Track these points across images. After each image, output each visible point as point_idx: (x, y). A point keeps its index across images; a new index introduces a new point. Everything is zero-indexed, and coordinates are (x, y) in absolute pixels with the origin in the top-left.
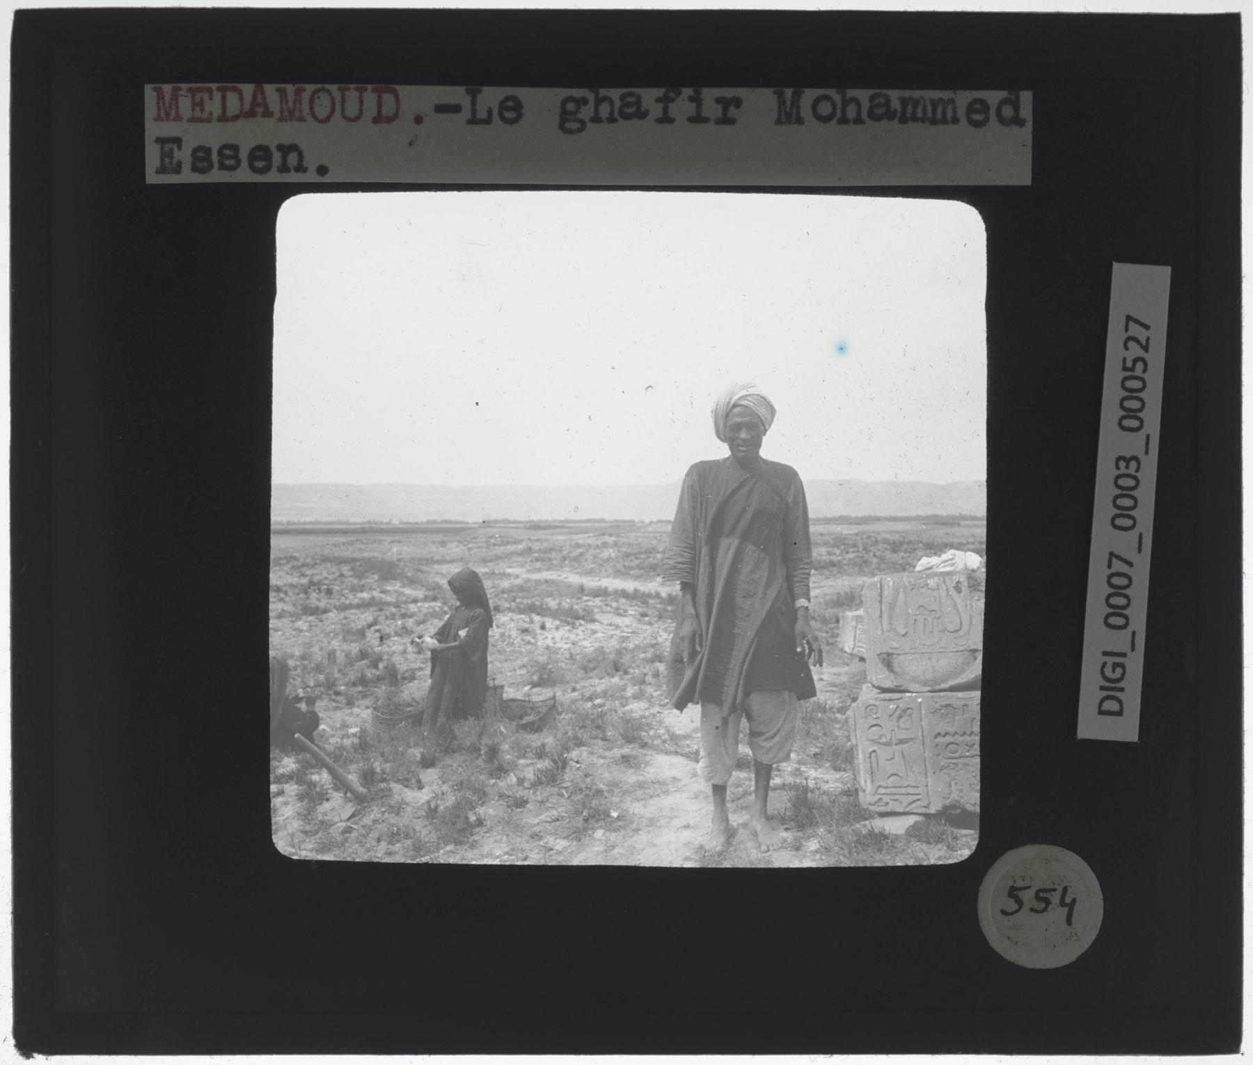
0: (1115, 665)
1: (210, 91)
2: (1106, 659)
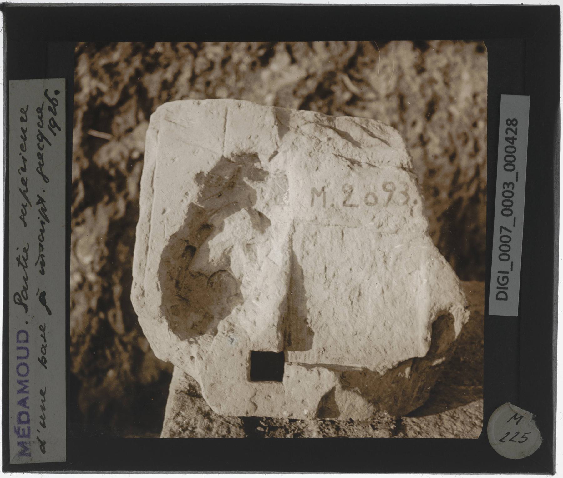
0: (504, 278)
2: (500, 274)
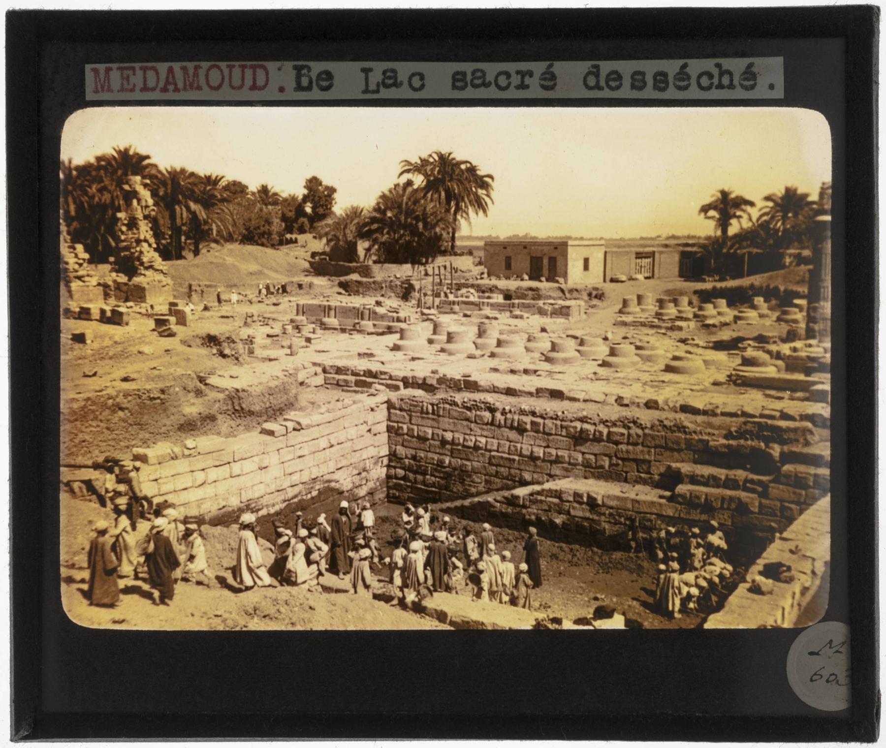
1: (133, 69)
